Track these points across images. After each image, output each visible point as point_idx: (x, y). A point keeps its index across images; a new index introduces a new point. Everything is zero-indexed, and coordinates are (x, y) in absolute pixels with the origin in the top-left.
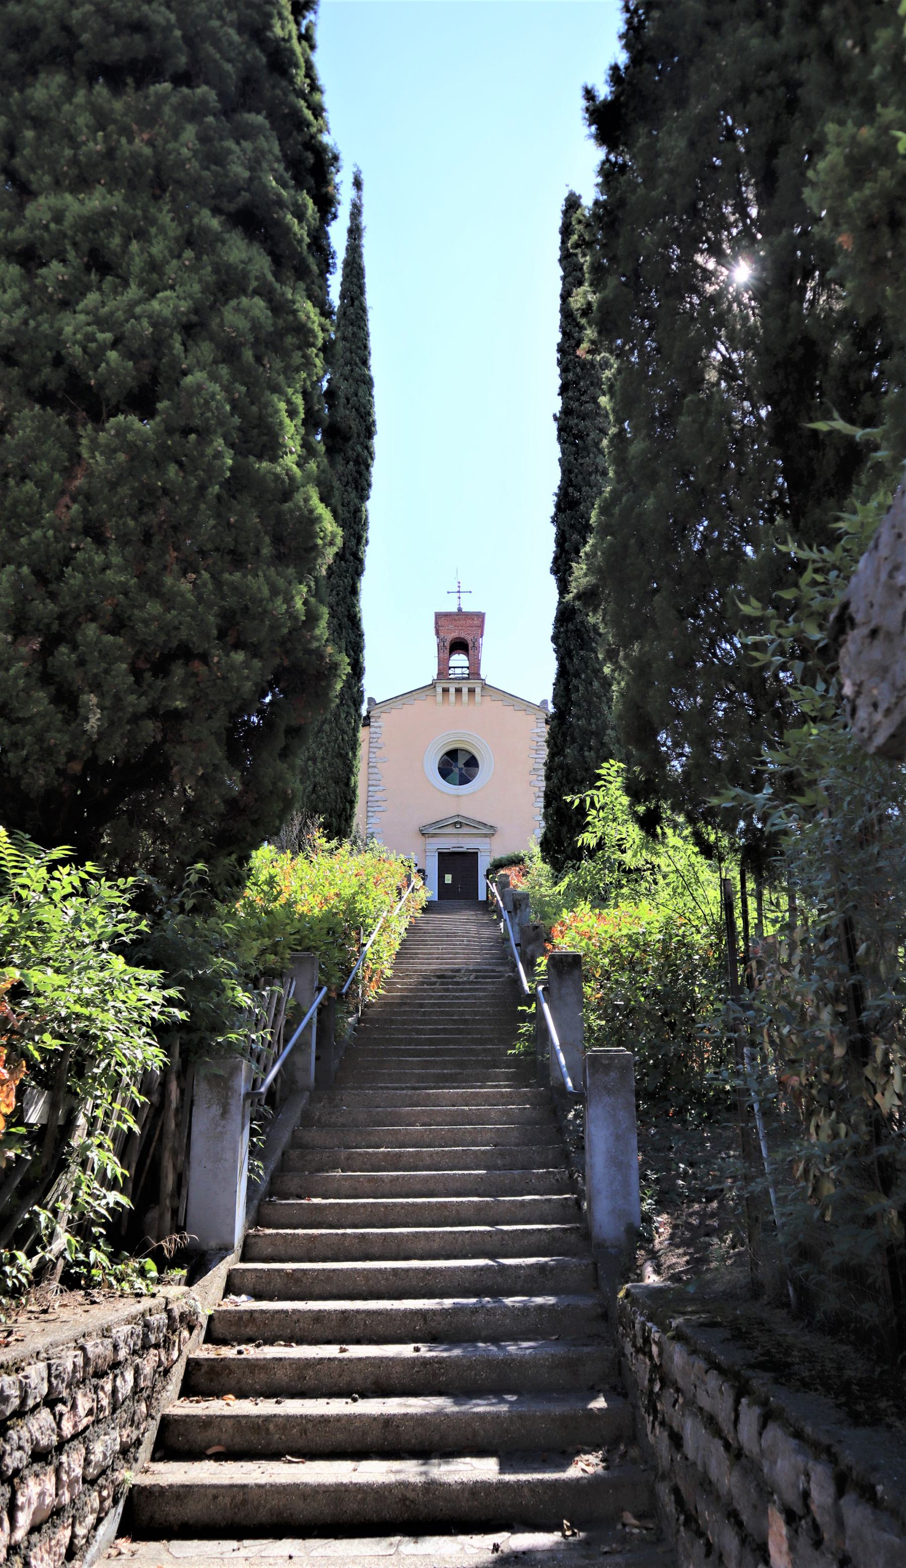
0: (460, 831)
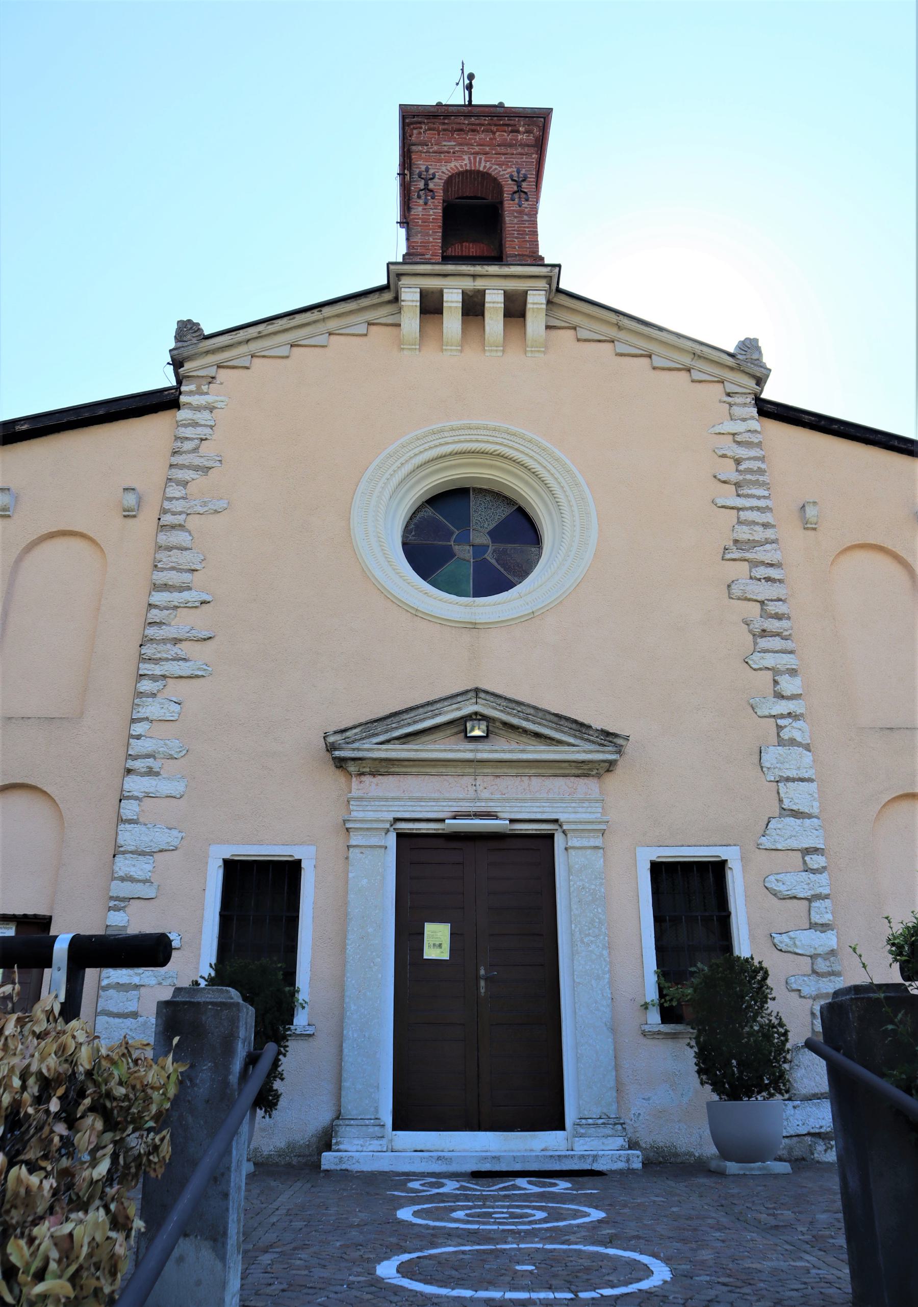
0: (484, 752)
